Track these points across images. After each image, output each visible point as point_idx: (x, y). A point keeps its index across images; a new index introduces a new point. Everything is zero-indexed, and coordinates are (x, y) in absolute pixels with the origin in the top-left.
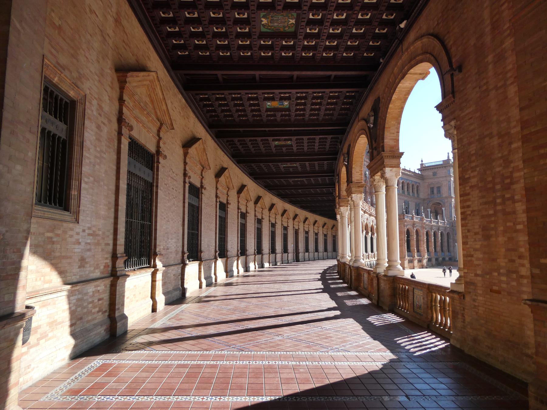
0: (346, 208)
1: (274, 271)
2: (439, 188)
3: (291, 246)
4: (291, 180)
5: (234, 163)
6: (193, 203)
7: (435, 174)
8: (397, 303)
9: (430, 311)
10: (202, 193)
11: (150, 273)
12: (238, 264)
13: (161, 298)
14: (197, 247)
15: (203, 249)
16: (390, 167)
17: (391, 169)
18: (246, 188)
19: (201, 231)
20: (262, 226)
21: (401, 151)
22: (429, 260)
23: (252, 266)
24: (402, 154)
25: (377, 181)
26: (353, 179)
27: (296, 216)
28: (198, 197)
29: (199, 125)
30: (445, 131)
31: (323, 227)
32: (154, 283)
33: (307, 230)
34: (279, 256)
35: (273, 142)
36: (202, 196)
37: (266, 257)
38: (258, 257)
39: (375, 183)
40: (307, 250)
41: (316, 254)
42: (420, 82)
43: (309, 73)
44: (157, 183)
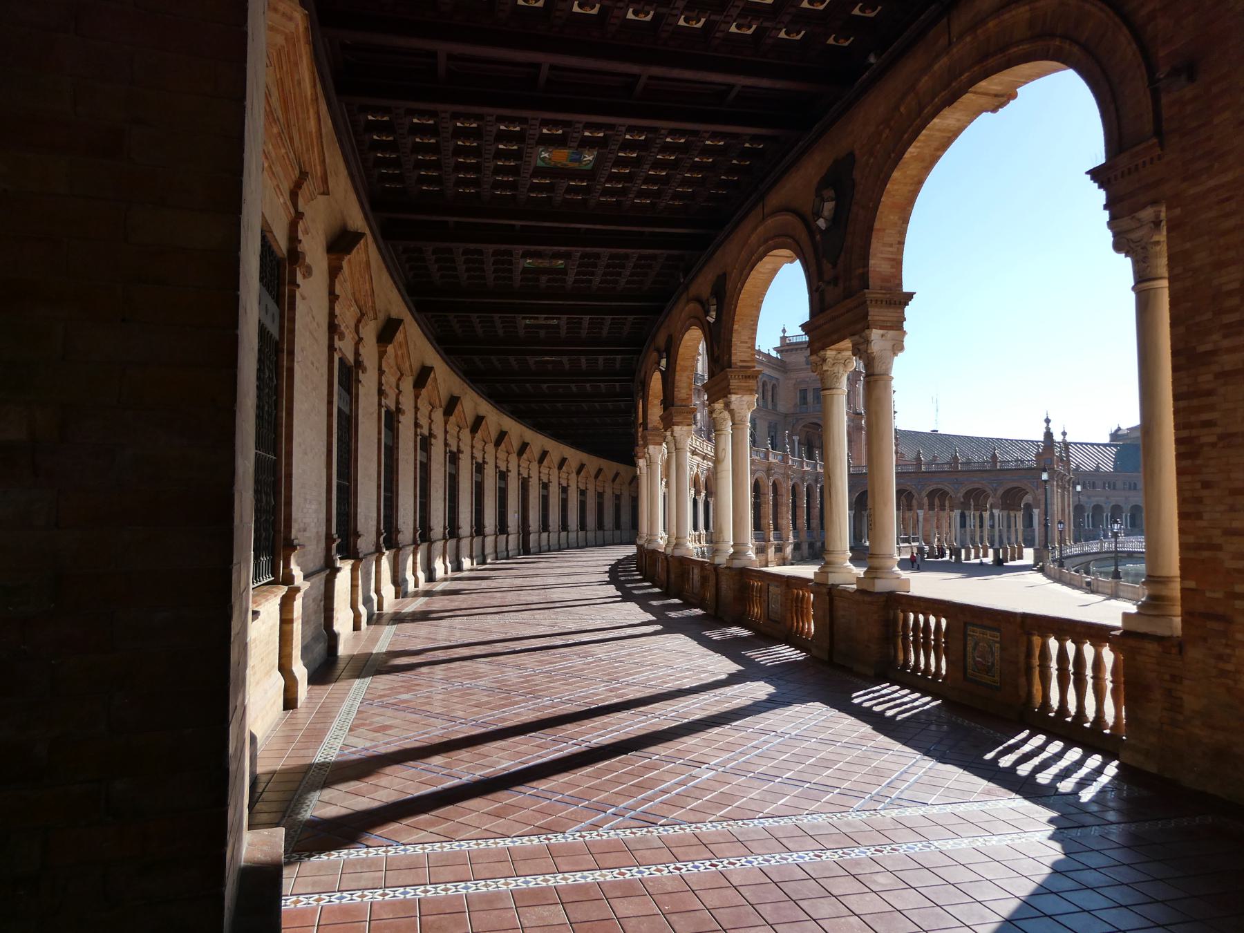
0: (685, 428)
1: (496, 578)
3: (513, 519)
4: (531, 360)
5: (410, 310)
8: (896, 656)
9: (1023, 680)
10: (358, 381)
11: (278, 601)
12: (414, 563)
13: (300, 670)
15: (360, 528)
16: (882, 328)
18: (432, 375)
19: (356, 480)
20: (457, 470)
21: (906, 289)
22: (797, 547)
23: (439, 565)
24: (910, 296)
26: (734, 358)
27: (524, 447)
29: (353, 197)
30: (1114, 236)
31: (578, 473)
32: (286, 627)
33: (546, 480)
34: (490, 541)
35: (521, 261)
37: (465, 544)
38: (451, 543)
39: (825, 368)
40: (545, 527)
41: (564, 534)
42: (986, 117)
43: (688, 74)
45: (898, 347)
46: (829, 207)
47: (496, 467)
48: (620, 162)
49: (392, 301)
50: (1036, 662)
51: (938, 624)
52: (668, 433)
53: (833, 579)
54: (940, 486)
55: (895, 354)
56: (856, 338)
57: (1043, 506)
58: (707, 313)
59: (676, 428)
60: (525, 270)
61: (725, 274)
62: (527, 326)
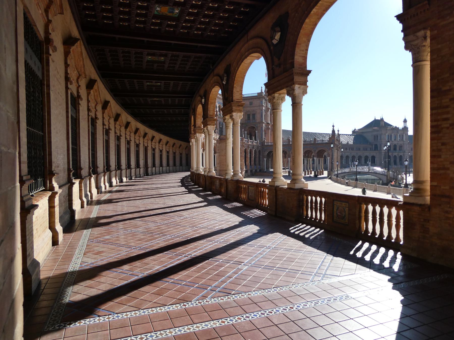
1: (137, 185)
2: (254, 115)
3: (142, 162)
4: (149, 100)
7: (251, 104)
8: (303, 213)
9: (357, 222)
10: (79, 104)
11: (47, 198)
12: (104, 180)
13: (59, 228)
16: (299, 84)
17: (299, 86)
18: (109, 104)
19: (80, 146)
20: (120, 143)
21: (308, 69)
22: (246, 172)
23: (114, 181)
24: (310, 72)
26: (234, 98)
27: (145, 135)
29: (74, 23)
30: (405, 44)
31: (166, 145)
32: (52, 210)
34: (133, 171)
36: (79, 107)
37: (124, 172)
38: (118, 172)
39: (274, 101)
40: (154, 165)
41: (161, 168)
44: (48, 81)
45: (305, 92)
47: (135, 142)
48: (190, 14)
50: (363, 214)
51: (321, 201)
52: (205, 129)
53: (277, 184)
55: (304, 95)
56: (289, 88)
57: (331, 156)
58: (222, 80)
59: (209, 126)
60: (148, 61)
62: (148, 85)
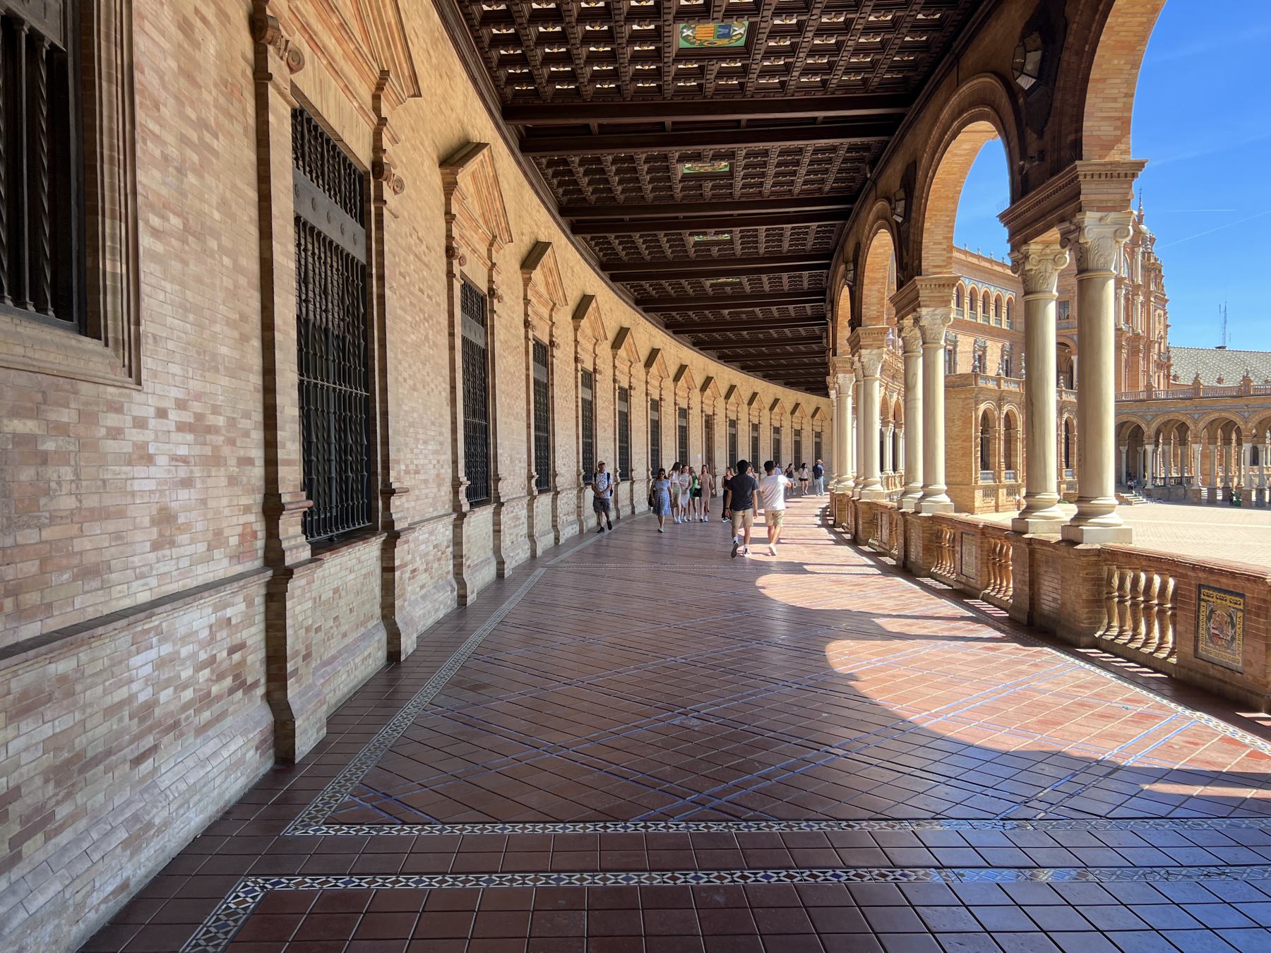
0: (875, 351)
5: (564, 231)
6: (471, 338)
14: (487, 465)
15: (502, 471)
16: (1099, 209)
17: (1099, 215)
18: (593, 304)
25: (1034, 258)
28: (484, 324)
35: (679, 166)
36: (492, 320)
39: (1027, 267)
44: (381, 266)
46: (1033, 59)
48: (776, 32)
49: (533, 217)
52: (856, 358)
54: (1224, 414)
56: (1066, 225)
59: (863, 352)
60: (686, 177)
61: (915, 162)
62: (696, 244)
